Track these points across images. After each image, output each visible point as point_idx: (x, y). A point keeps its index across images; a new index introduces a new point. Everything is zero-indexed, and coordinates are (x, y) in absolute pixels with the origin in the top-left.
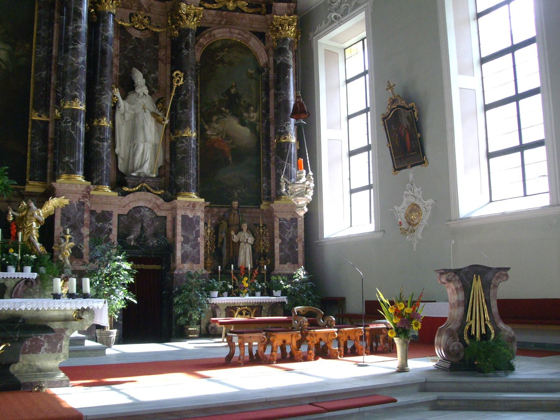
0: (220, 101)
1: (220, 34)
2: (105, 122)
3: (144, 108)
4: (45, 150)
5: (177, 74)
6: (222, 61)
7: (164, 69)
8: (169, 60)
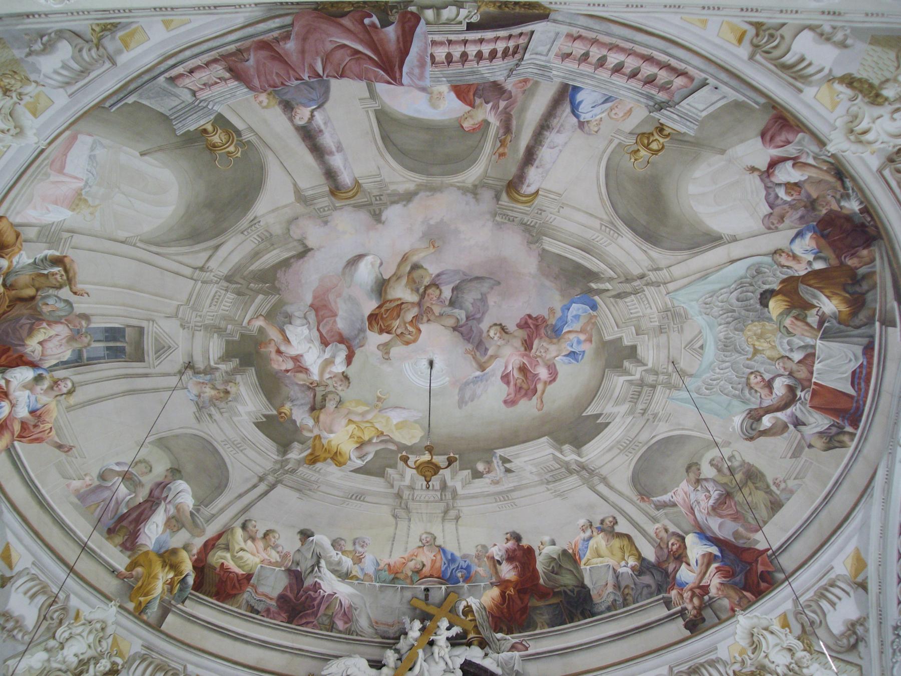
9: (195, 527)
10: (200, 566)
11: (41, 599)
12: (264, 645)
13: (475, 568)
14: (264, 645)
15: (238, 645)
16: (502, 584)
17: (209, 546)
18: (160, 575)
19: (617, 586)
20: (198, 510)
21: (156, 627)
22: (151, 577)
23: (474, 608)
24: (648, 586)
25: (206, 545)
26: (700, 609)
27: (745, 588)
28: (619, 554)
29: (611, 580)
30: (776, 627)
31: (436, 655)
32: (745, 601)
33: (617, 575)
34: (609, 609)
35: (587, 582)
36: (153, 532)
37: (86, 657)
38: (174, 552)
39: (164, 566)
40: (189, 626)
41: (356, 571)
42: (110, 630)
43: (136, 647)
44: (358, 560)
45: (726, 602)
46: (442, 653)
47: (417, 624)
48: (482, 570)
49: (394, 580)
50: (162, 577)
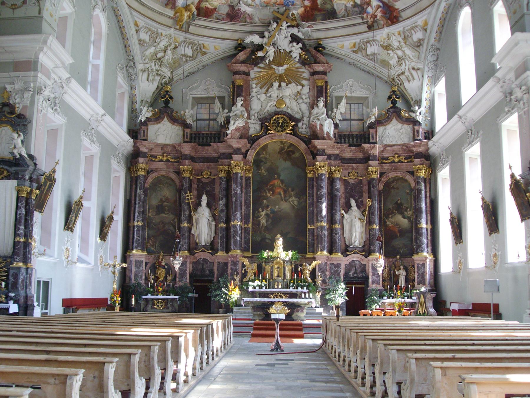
0: (393, 207)
1: (392, 175)
2: (338, 226)
3: (355, 217)
4: (314, 240)
6: (393, 188)
8: (367, 192)
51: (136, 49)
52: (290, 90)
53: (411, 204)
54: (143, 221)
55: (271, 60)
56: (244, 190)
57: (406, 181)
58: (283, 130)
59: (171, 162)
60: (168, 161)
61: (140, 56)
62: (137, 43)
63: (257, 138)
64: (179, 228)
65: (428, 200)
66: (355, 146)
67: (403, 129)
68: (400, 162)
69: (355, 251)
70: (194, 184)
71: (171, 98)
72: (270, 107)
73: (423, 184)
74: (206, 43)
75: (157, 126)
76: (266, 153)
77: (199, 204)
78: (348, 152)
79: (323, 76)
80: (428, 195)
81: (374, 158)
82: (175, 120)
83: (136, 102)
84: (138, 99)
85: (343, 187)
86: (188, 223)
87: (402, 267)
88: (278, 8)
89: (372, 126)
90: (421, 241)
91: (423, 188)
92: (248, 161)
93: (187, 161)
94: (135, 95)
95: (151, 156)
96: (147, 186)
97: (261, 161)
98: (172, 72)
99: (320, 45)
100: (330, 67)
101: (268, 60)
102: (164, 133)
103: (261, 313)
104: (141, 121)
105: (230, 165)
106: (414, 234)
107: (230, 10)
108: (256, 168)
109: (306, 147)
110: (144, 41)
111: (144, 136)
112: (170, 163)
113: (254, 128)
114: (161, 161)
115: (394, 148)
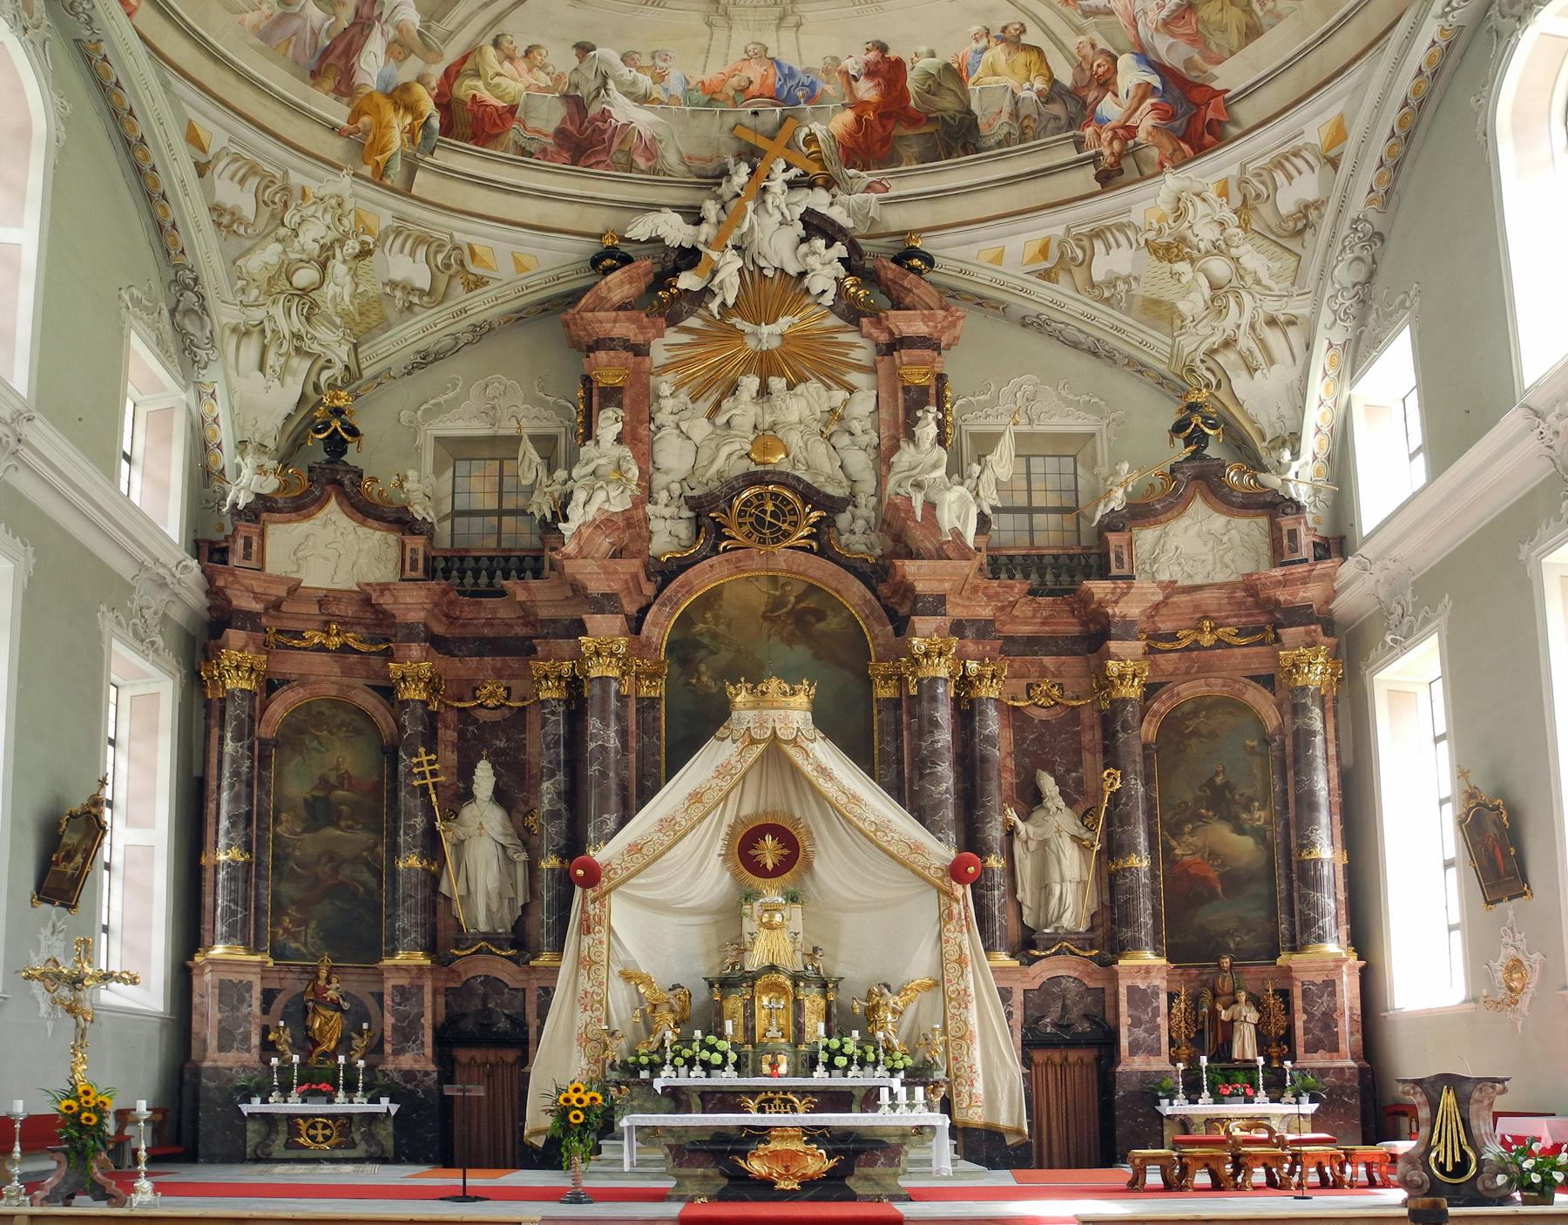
0: (1196, 799)
1: (1188, 690)
5: (1109, 775)
6: (1196, 733)
7: (1091, 760)
8: (1099, 748)
9: (425, 45)
10: (445, 103)
11: (253, 182)
12: (545, 195)
13: (820, 86)
14: (545, 195)
15: (513, 199)
16: (858, 106)
17: (452, 74)
18: (395, 122)
19: (1015, 115)
20: (428, 28)
21: (406, 192)
22: (382, 127)
23: (819, 136)
24: (1057, 118)
25: (447, 73)
26: (1119, 157)
27: (1182, 138)
28: (1022, 72)
29: (1007, 106)
30: (1211, 194)
31: (770, 206)
32: (1179, 155)
33: (1016, 101)
34: (1000, 144)
35: (974, 106)
36: (372, 64)
37: (327, 240)
38: (406, 88)
39: (396, 110)
40: (446, 184)
41: (657, 92)
42: (349, 204)
43: (386, 220)
44: (660, 78)
45: (1155, 153)
46: (777, 202)
47: (744, 168)
48: (831, 88)
49: (711, 101)
50: (397, 126)
51: (205, 247)
52: (803, 402)
53: (1267, 787)
54: (247, 847)
55: (730, 302)
56: (633, 743)
57: (1245, 708)
58: (780, 536)
59: (358, 652)
60: (345, 649)
61: (221, 274)
62: (206, 219)
63: (682, 565)
64: (394, 872)
65: (1334, 771)
66: (1051, 593)
67: (1234, 532)
68: (1220, 644)
69: (1060, 943)
70: (447, 727)
71: (354, 432)
72: (729, 459)
73: (1316, 712)
74: (479, 243)
75: (299, 529)
76: (716, 618)
77: (468, 796)
78: (1028, 618)
79: (929, 352)
80: (1332, 751)
81: (1128, 630)
82: (366, 509)
83: (219, 446)
84: (225, 434)
85: (1009, 735)
86: (422, 857)
87: (1243, 996)
88: (755, 113)
89: (1113, 523)
90: (1314, 906)
91: (1318, 725)
92: (648, 644)
93: (414, 646)
94: (215, 420)
95: (279, 632)
96: (265, 731)
97: (699, 646)
98: (356, 346)
99: (913, 253)
100: (953, 325)
101: (718, 301)
102: (327, 553)
103: (711, 1172)
104: (235, 505)
105: (578, 657)
106: (1282, 886)
107: (570, 117)
108: (677, 669)
109: (869, 595)
110: (236, 217)
111: (247, 556)
112: (353, 658)
113: (668, 532)
114: (321, 648)
115: (1197, 596)
